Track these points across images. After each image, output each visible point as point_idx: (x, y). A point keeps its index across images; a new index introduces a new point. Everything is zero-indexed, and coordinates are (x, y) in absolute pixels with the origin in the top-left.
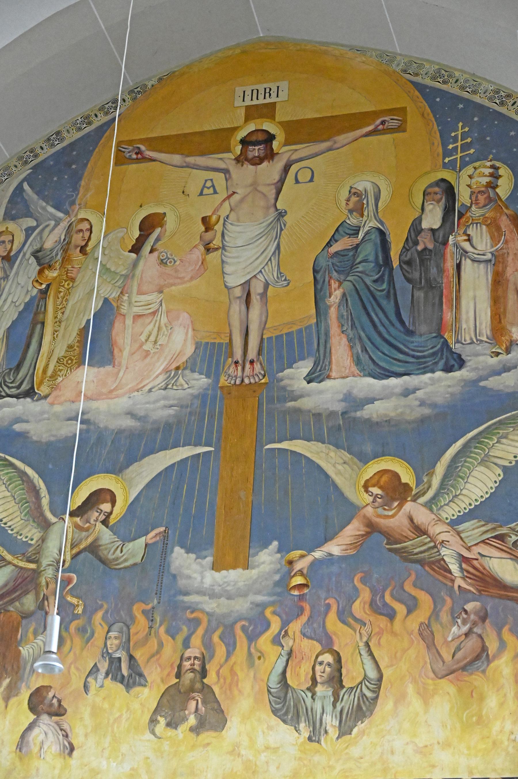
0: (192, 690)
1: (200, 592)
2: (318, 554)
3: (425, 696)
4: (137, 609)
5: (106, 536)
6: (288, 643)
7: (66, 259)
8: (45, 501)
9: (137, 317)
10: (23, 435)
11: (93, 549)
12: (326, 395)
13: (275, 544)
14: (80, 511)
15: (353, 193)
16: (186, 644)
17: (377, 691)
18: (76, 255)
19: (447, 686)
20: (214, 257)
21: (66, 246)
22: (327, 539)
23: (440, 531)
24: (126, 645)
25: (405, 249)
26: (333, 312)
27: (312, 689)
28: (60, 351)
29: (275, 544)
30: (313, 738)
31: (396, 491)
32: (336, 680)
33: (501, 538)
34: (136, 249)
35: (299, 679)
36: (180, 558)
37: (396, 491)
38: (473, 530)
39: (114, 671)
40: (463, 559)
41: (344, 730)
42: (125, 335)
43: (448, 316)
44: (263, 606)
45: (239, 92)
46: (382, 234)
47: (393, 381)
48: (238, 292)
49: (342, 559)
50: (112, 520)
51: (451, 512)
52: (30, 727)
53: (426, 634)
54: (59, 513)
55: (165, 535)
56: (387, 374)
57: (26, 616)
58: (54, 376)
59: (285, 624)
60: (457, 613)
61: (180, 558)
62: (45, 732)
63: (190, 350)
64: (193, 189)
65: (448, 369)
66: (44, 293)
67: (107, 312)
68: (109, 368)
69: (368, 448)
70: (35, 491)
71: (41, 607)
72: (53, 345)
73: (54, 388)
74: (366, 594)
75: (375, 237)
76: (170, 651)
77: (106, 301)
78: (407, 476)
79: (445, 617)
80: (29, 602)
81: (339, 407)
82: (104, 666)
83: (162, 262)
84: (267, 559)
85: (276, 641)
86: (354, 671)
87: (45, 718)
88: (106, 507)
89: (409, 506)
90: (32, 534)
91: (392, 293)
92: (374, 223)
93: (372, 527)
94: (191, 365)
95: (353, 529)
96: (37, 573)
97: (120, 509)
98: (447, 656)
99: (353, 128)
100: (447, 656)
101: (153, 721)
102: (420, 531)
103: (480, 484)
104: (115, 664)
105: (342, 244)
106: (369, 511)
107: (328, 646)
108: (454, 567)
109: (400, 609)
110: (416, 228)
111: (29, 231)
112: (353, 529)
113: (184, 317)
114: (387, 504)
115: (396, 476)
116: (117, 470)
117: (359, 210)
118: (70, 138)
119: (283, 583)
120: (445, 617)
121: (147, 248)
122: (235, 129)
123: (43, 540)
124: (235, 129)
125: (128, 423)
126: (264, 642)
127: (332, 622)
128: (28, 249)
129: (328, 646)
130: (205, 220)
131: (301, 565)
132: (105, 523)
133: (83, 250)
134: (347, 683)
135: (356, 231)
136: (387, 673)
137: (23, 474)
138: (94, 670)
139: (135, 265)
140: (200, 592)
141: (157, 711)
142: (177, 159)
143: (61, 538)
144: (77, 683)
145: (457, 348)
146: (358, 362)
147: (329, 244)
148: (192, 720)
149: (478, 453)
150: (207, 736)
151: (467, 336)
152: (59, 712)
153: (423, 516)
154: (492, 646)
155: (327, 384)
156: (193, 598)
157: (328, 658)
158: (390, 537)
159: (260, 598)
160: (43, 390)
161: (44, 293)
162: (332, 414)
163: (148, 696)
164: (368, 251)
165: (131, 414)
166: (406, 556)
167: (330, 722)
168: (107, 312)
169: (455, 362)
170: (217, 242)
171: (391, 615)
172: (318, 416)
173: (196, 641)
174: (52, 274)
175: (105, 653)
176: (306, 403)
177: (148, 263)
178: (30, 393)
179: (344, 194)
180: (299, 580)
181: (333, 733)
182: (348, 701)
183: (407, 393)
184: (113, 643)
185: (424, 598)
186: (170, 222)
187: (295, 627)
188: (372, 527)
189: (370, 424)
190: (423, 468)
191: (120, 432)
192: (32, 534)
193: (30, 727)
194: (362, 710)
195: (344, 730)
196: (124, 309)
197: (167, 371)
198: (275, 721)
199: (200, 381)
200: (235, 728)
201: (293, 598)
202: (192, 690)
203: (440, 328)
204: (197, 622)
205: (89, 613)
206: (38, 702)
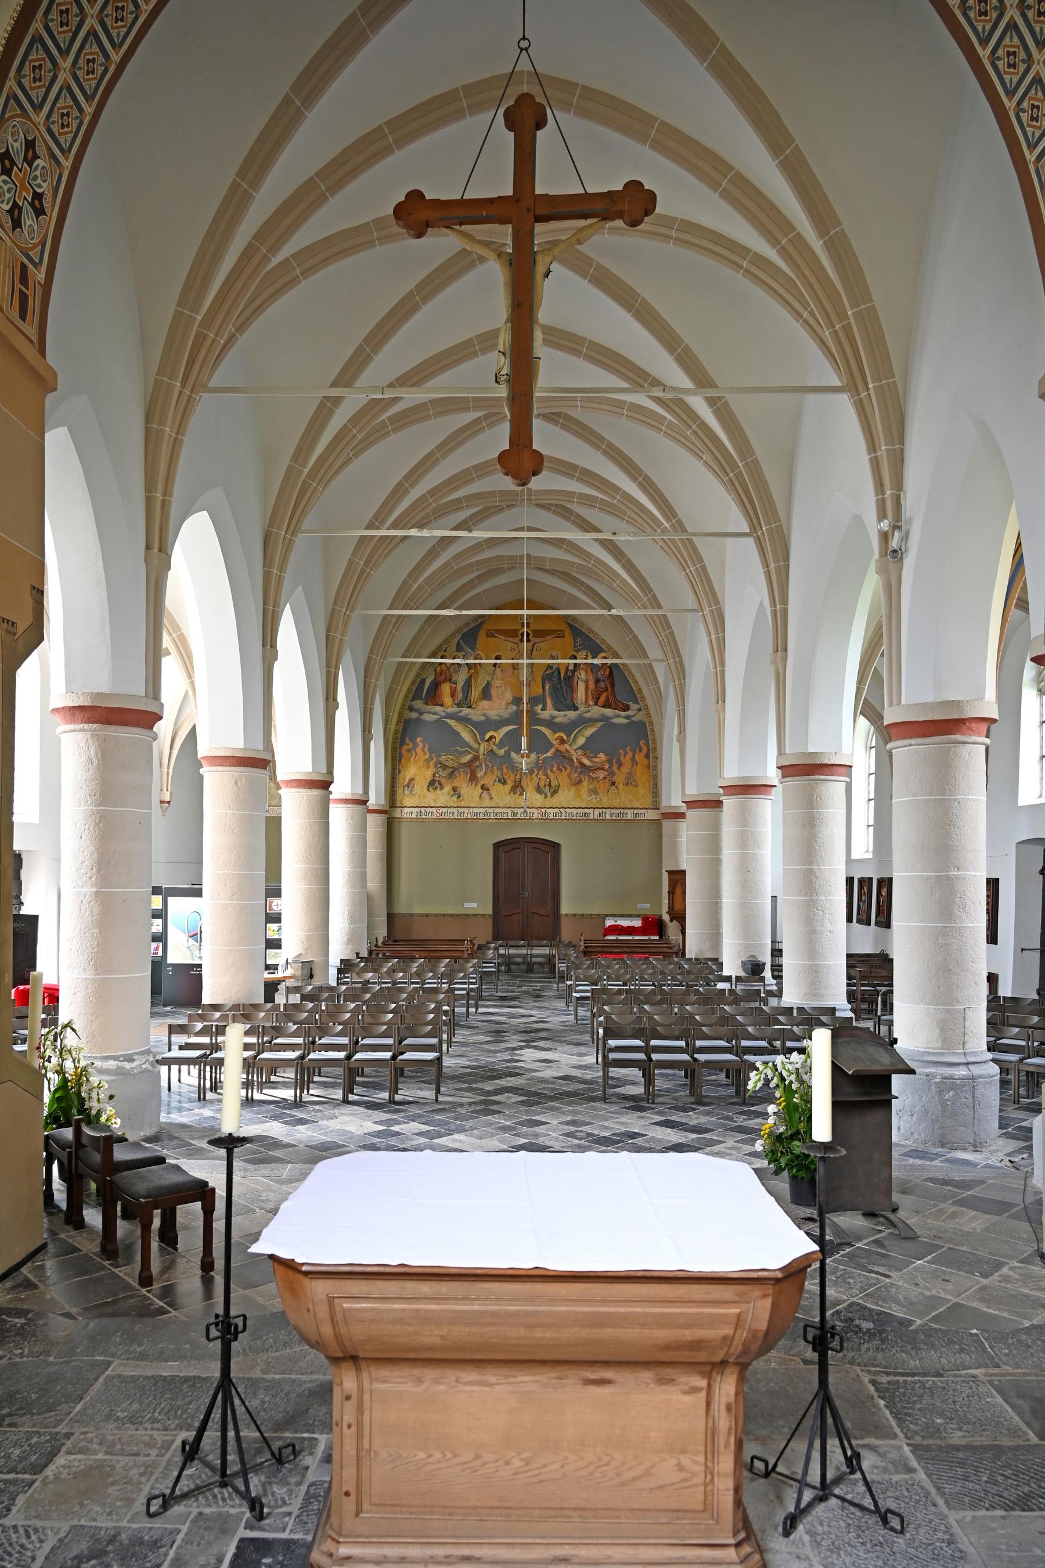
5: (495, 748)
11: (492, 751)
12: (546, 715)
19: (573, 788)
31: (562, 741)
32: (550, 785)
35: (542, 785)
37: (562, 741)
38: (579, 752)
39: (500, 781)
42: (494, 692)
51: (575, 747)
53: (569, 776)
60: (576, 771)
64: (509, 649)
66: (470, 677)
67: (488, 686)
72: (475, 693)
76: (512, 777)
78: (565, 738)
80: (477, 763)
86: (554, 783)
90: (476, 746)
91: (561, 687)
93: (557, 750)
94: (512, 703)
95: (553, 750)
97: (497, 741)
102: (568, 751)
103: (581, 741)
112: (553, 750)
116: (496, 730)
119: (537, 762)
129: (548, 777)
143: (483, 748)
152: (488, 790)
153: (568, 748)
158: (561, 753)
163: (508, 787)
164: (555, 675)
166: (565, 757)
167: (549, 794)
168: (488, 686)
169: (576, 709)
176: (541, 716)
178: (470, 707)
188: (557, 750)
189: (556, 724)
190: (569, 736)
192: (476, 746)
194: (555, 792)
206: (483, 787)
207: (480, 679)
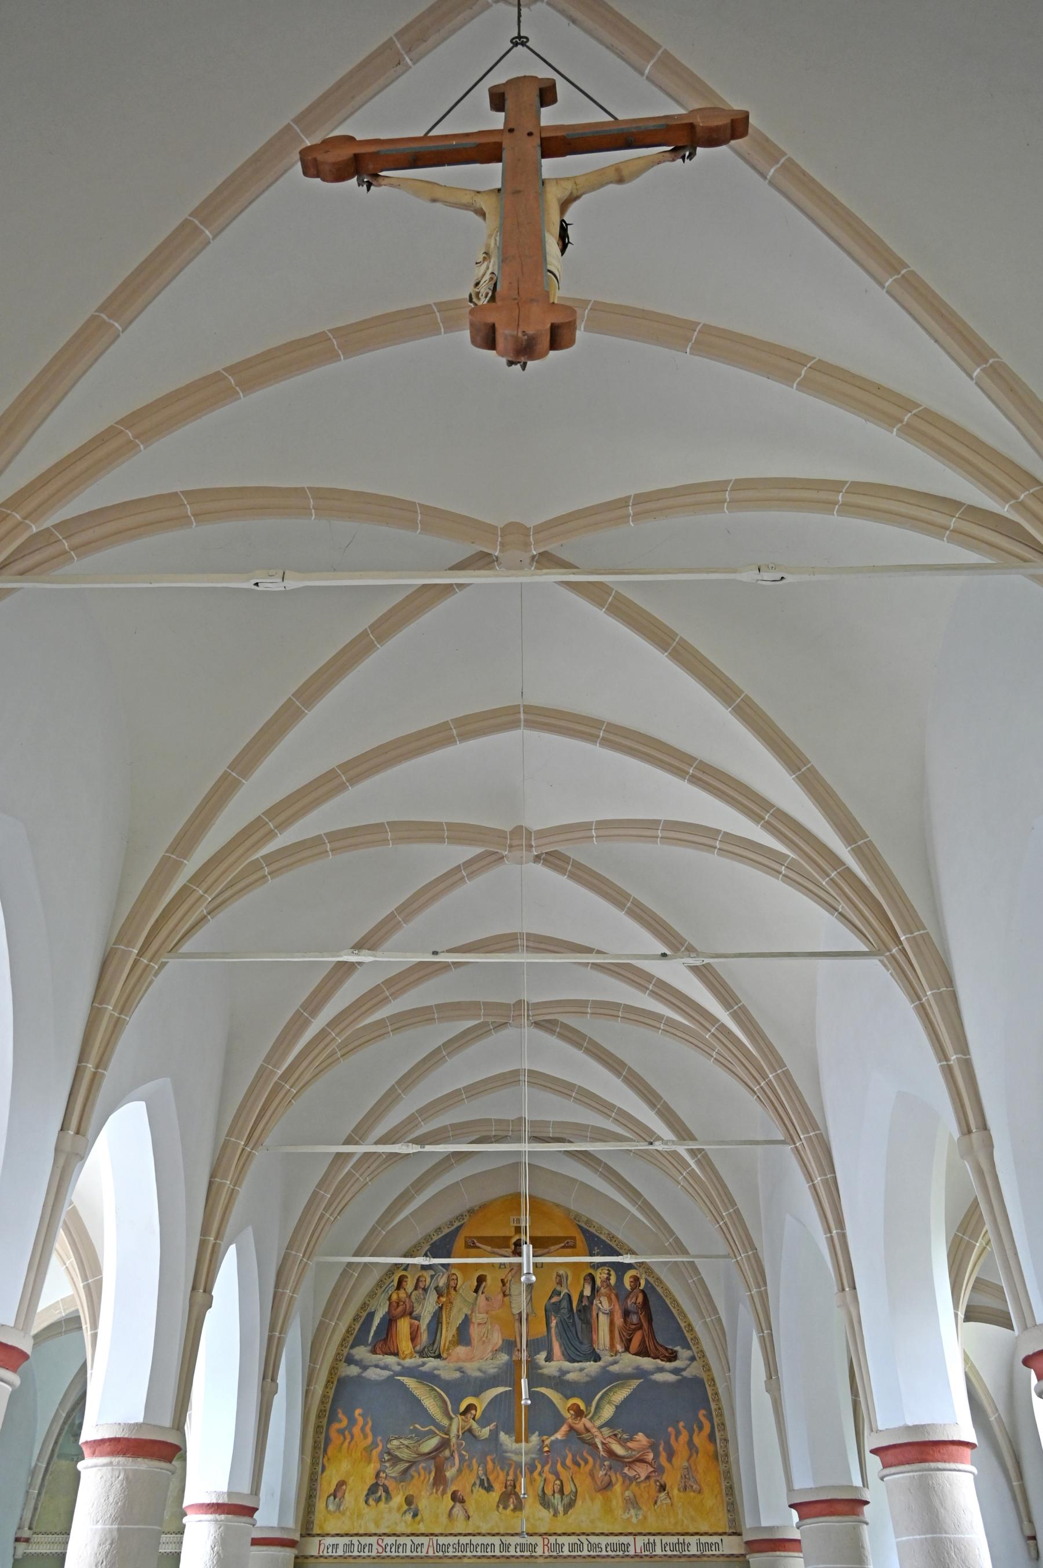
0: (511, 1494)
1: (512, 1452)
2: (553, 1438)
3: (592, 1499)
4: (489, 1458)
5: (475, 1426)
6: (544, 1475)
7: (448, 1293)
8: (450, 1407)
9: (479, 1324)
10: (438, 1377)
11: (470, 1430)
12: (551, 1369)
13: (537, 1433)
14: (464, 1413)
15: (558, 1275)
16: (508, 1475)
17: (576, 1496)
18: (453, 1292)
19: (599, 1496)
20: (506, 1299)
21: (448, 1286)
22: (556, 1432)
23: (594, 1430)
24: (486, 1474)
25: (578, 1305)
26: (553, 1330)
27: (553, 1495)
28: (450, 1338)
29: (537, 1433)
30: (555, 1514)
31: (579, 1413)
32: (561, 1491)
33: (615, 1435)
34: (476, 1291)
35: (549, 1491)
36: (503, 1437)
37: (579, 1413)
38: (606, 1431)
39: (482, 1484)
40: (603, 1444)
41: (566, 1512)
42: (475, 1332)
43: (595, 1337)
44: (534, 1460)
45: (512, 1218)
46: (569, 1296)
47: (576, 1364)
48: (517, 1317)
49: (561, 1441)
50: (477, 1418)
51: (598, 1423)
52: (453, 1507)
53: (592, 1474)
54: (456, 1411)
55: (497, 1426)
56: (573, 1361)
57: (447, 1459)
58: (448, 1349)
59: (543, 1467)
60: (602, 1465)
61: (503, 1437)
62: (458, 1509)
63: (500, 1342)
65: (595, 1361)
66: (441, 1308)
67: (467, 1321)
68: (469, 1348)
69: (569, 1393)
70: (444, 1402)
71: (452, 1455)
72: (447, 1333)
73: (449, 1355)
74: (570, 1456)
75: (567, 1297)
76: (502, 1476)
77: (466, 1315)
78: (583, 1407)
79: (597, 1467)
80: (447, 1453)
81: (557, 1374)
82: (478, 1482)
83: (487, 1299)
84: (535, 1438)
85: (540, 1474)
86: (568, 1488)
87: (458, 1504)
88: (473, 1412)
89: (584, 1419)
90: (445, 1422)
91: (574, 1324)
92: (566, 1291)
93: (571, 1428)
94: (500, 1350)
95: (564, 1428)
96: (449, 1440)
97: (479, 1414)
98: (599, 1483)
99: (554, 1244)
100: (599, 1483)
101: (498, 1506)
102: (588, 1430)
103: (608, 1412)
104: (482, 1481)
105: (554, 1300)
106: (570, 1420)
107: (558, 1478)
108: (600, 1446)
109: (582, 1463)
110: (581, 1295)
111: (432, 1277)
112: (564, 1428)
113: (497, 1327)
114: (575, 1418)
115: (578, 1406)
116: (476, 1395)
117: (560, 1283)
118: (446, 1231)
119: (541, 1450)
120: (597, 1467)
121: (480, 1292)
122: (511, 1237)
123: (450, 1425)
124: (511, 1237)
125: (478, 1374)
126: (536, 1474)
127: (559, 1467)
128: (433, 1286)
129: (558, 1478)
130: (502, 1280)
131: (547, 1442)
132: (474, 1419)
133: (455, 1288)
134: (566, 1493)
135: (559, 1294)
136: (579, 1489)
137: (440, 1395)
138: (474, 1484)
139: (476, 1299)
140: (512, 1452)
141: (499, 1502)
142: (489, 1248)
143: (456, 1425)
144: (468, 1489)
145: (598, 1351)
146: (563, 1354)
147: (550, 1298)
148: (512, 1506)
149: (607, 1399)
150: (517, 1513)
151: (601, 1347)
152: (462, 1501)
153: (589, 1425)
154: (614, 1479)
155: (552, 1363)
156: (508, 1455)
157: (558, 1482)
158: (578, 1433)
159: (534, 1456)
160: (444, 1355)
161: (441, 1308)
162: (555, 1377)
163: (495, 1496)
164: (565, 1304)
165: (480, 1370)
166: (583, 1441)
167: (561, 1509)
168: (467, 1321)
169: (597, 1358)
170: (507, 1292)
171: (579, 1465)
172: (549, 1377)
173: (511, 1473)
174: (443, 1299)
175: (478, 1477)
176: (545, 1371)
177: (482, 1298)
178: (439, 1356)
179: (555, 1275)
180: (546, 1449)
181: (562, 1513)
182: (566, 1500)
183: (582, 1370)
184: (481, 1472)
185: (591, 1460)
186: (489, 1279)
187: (547, 1468)
188: (571, 1428)
189: (568, 1383)
190: (588, 1404)
191: (476, 1378)
192: (445, 1422)
193: (453, 1507)
194: (570, 1505)
195: (566, 1512)
196: (473, 1320)
197: (492, 1351)
198: (541, 1507)
199: (504, 1358)
200: (527, 1510)
201: (545, 1456)
202: (511, 1494)
203: (591, 1342)
204: (510, 1466)
205: (471, 1458)
206: (455, 1497)
207: (454, 1311)
